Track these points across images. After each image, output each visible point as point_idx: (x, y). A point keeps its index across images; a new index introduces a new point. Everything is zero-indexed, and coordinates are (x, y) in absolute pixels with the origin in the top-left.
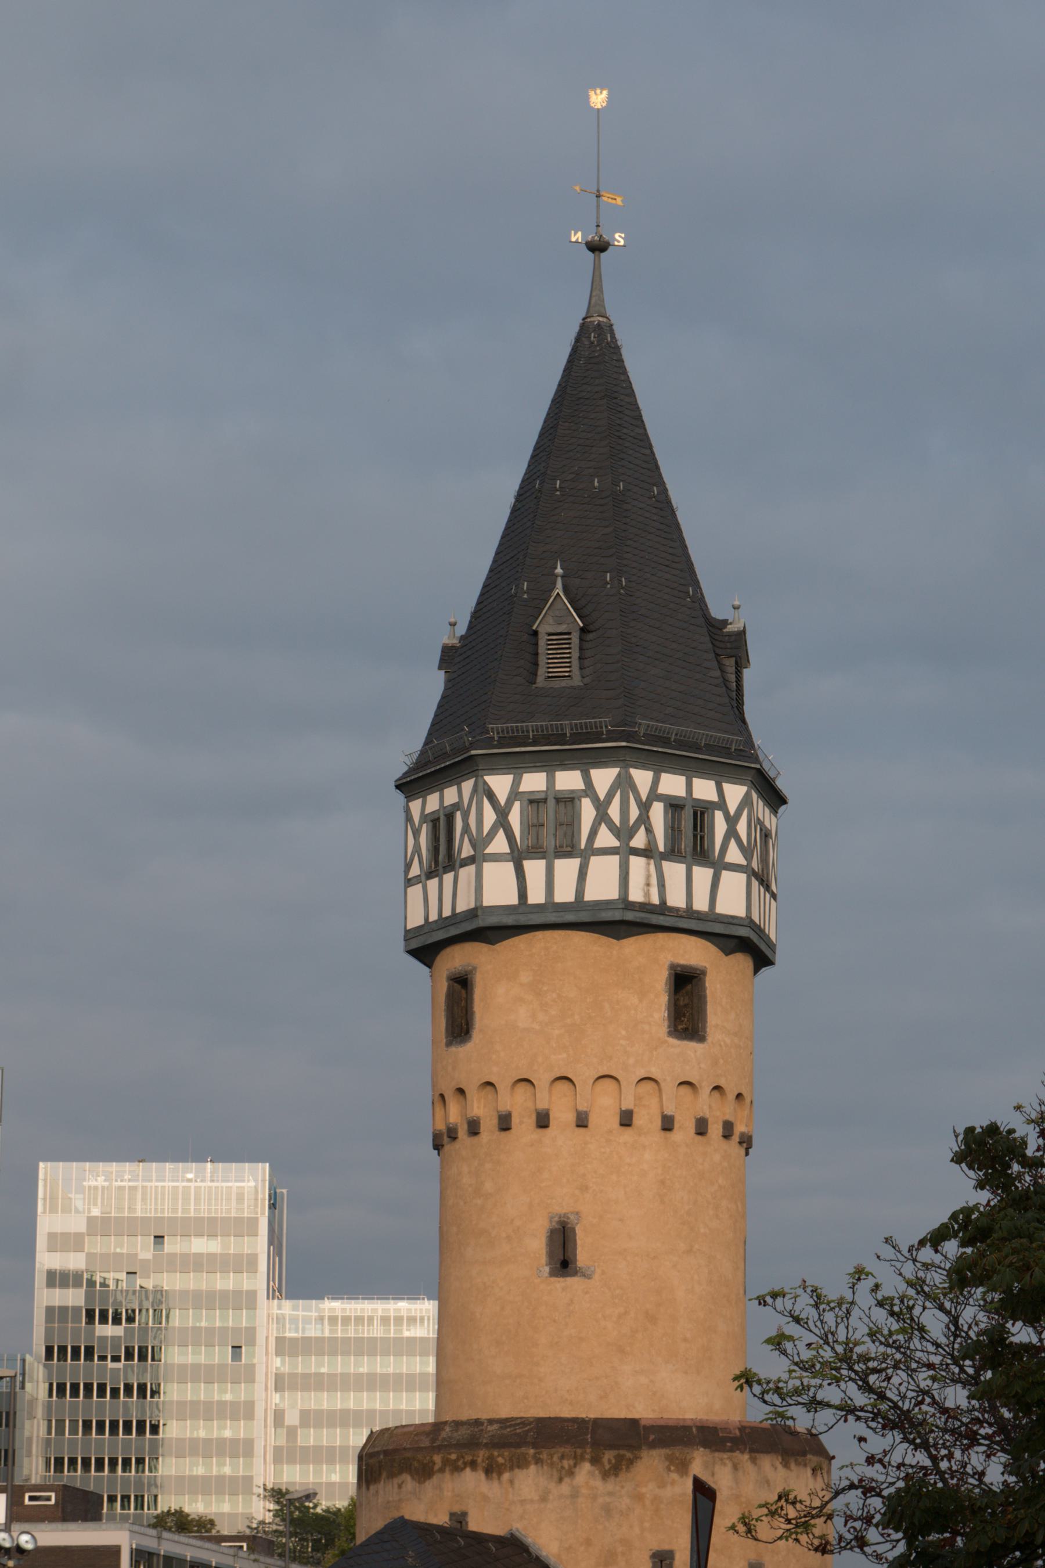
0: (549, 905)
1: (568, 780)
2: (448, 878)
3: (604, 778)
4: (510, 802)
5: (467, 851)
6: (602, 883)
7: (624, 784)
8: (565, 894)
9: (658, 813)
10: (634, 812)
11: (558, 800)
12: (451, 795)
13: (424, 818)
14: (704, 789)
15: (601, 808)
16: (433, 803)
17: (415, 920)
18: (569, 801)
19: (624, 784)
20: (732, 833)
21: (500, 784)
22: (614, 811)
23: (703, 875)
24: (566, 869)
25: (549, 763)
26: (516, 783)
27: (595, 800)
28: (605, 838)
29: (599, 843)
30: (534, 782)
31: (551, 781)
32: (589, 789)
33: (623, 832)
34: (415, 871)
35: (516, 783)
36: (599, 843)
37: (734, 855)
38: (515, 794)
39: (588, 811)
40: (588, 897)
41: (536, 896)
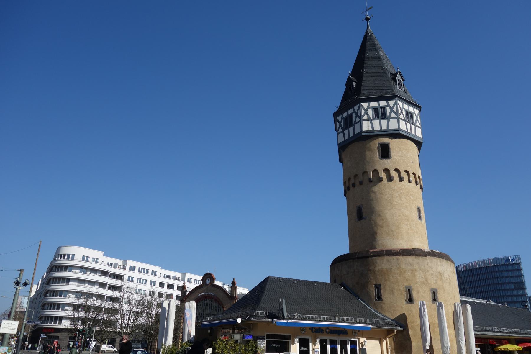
0: (381, 130)
1: (383, 103)
2: (351, 129)
3: (391, 103)
4: (367, 109)
5: (358, 119)
6: (393, 125)
7: (396, 104)
8: (384, 127)
9: (404, 111)
10: (399, 111)
11: (381, 108)
12: (351, 111)
13: (342, 119)
14: (411, 109)
15: (392, 109)
16: (345, 115)
17: (341, 140)
18: (384, 108)
19: (396, 104)
20: (417, 119)
21: (365, 105)
22: (395, 109)
23: (413, 126)
24: (384, 122)
25: (378, 100)
26: (369, 105)
27: (390, 108)
28: (393, 115)
29: (391, 117)
30: (374, 104)
31: (379, 104)
32: (388, 105)
33: (397, 114)
34: (340, 130)
35: (369, 105)
36: (391, 117)
37: (418, 124)
38: (369, 107)
39: (388, 110)
40: (390, 128)
41: (377, 127)
